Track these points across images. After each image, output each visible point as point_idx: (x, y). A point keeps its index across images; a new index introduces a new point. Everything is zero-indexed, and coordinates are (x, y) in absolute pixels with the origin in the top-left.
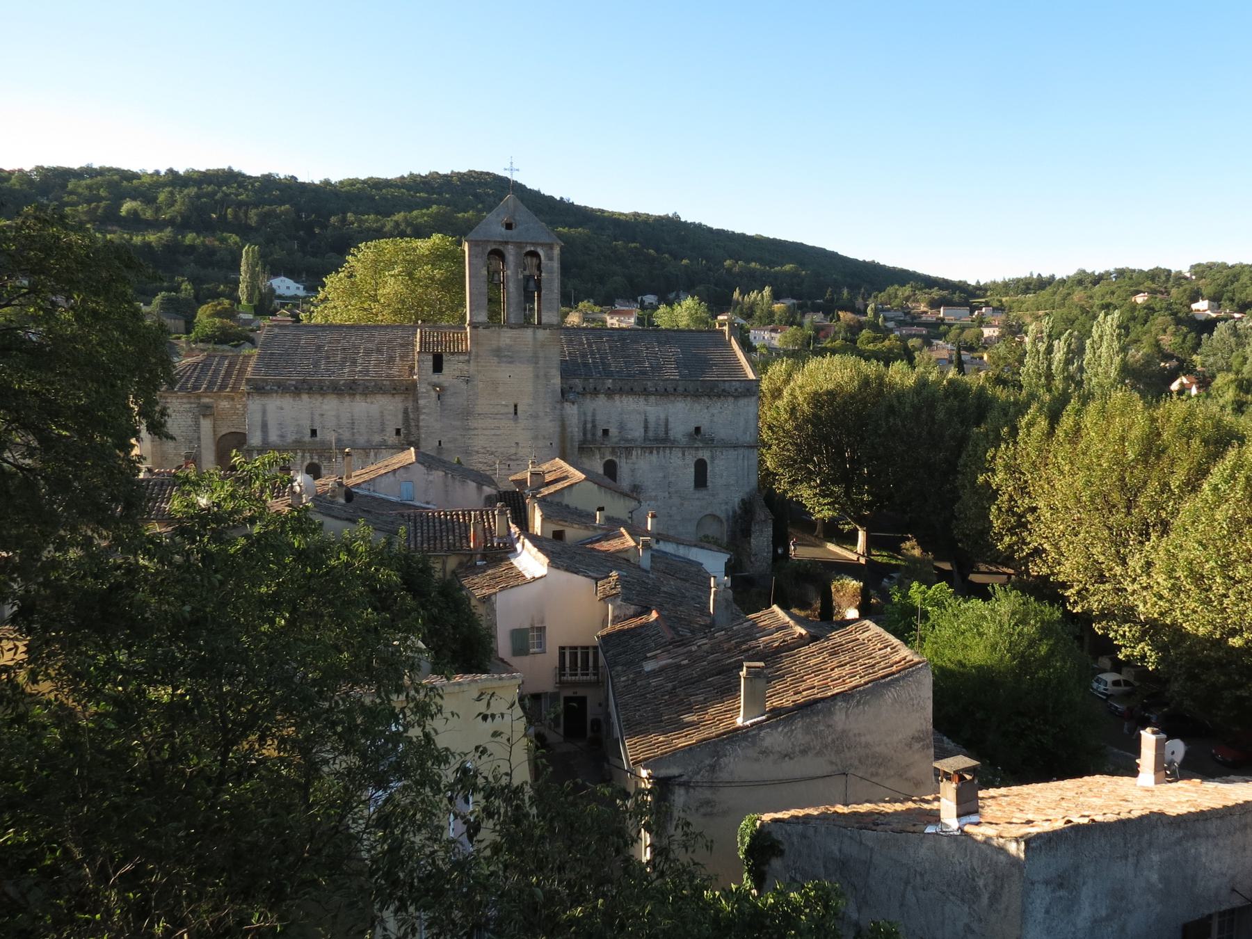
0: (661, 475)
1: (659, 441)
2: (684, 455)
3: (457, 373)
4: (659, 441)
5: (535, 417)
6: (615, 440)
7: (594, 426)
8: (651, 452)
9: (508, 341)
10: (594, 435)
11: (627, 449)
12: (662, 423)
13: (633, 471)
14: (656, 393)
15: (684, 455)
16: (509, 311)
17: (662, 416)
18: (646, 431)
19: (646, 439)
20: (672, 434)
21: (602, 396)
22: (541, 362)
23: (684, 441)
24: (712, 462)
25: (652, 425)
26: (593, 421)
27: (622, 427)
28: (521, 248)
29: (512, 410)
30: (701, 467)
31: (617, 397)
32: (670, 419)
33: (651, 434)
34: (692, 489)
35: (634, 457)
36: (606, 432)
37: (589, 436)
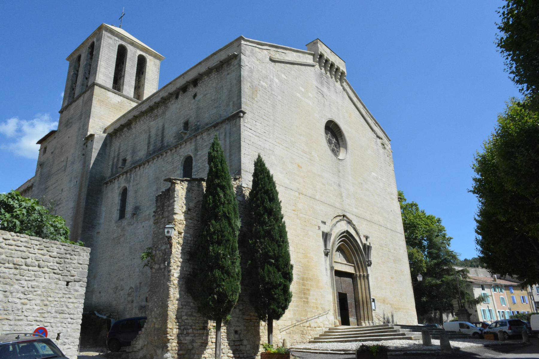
12: (160, 133)
13: (136, 192)
18: (148, 147)
24: (196, 155)
25: (152, 140)
32: (166, 126)
36: (125, 160)
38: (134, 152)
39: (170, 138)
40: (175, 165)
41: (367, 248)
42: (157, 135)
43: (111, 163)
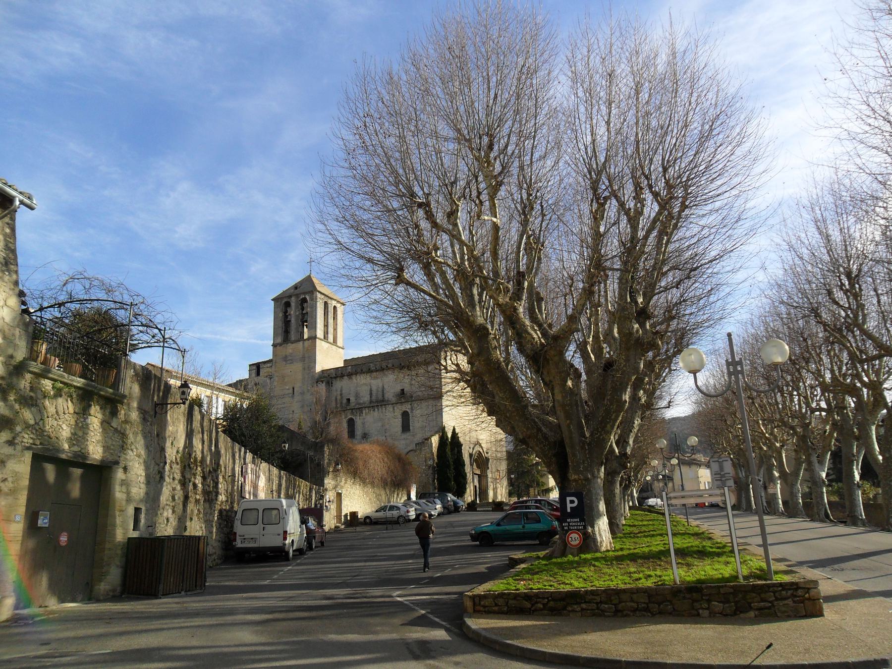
0: (380, 424)
1: (379, 402)
2: (394, 409)
3: (266, 374)
4: (379, 402)
5: (302, 393)
6: (353, 404)
7: (342, 398)
9: (290, 351)
10: (341, 403)
11: (360, 409)
12: (380, 390)
13: (363, 424)
14: (377, 371)
15: (394, 409)
16: (293, 336)
17: (381, 385)
18: (371, 397)
19: (371, 402)
20: (386, 396)
21: (346, 377)
23: (394, 400)
24: (412, 412)
25: (374, 393)
26: (341, 395)
27: (357, 396)
28: (298, 298)
29: (291, 391)
30: (405, 416)
31: (354, 377)
33: (374, 398)
34: (400, 433)
35: (364, 414)
36: (349, 400)
39: (390, 395)
40: (396, 414)
41: (487, 459)
42: (378, 391)
43: (334, 398)
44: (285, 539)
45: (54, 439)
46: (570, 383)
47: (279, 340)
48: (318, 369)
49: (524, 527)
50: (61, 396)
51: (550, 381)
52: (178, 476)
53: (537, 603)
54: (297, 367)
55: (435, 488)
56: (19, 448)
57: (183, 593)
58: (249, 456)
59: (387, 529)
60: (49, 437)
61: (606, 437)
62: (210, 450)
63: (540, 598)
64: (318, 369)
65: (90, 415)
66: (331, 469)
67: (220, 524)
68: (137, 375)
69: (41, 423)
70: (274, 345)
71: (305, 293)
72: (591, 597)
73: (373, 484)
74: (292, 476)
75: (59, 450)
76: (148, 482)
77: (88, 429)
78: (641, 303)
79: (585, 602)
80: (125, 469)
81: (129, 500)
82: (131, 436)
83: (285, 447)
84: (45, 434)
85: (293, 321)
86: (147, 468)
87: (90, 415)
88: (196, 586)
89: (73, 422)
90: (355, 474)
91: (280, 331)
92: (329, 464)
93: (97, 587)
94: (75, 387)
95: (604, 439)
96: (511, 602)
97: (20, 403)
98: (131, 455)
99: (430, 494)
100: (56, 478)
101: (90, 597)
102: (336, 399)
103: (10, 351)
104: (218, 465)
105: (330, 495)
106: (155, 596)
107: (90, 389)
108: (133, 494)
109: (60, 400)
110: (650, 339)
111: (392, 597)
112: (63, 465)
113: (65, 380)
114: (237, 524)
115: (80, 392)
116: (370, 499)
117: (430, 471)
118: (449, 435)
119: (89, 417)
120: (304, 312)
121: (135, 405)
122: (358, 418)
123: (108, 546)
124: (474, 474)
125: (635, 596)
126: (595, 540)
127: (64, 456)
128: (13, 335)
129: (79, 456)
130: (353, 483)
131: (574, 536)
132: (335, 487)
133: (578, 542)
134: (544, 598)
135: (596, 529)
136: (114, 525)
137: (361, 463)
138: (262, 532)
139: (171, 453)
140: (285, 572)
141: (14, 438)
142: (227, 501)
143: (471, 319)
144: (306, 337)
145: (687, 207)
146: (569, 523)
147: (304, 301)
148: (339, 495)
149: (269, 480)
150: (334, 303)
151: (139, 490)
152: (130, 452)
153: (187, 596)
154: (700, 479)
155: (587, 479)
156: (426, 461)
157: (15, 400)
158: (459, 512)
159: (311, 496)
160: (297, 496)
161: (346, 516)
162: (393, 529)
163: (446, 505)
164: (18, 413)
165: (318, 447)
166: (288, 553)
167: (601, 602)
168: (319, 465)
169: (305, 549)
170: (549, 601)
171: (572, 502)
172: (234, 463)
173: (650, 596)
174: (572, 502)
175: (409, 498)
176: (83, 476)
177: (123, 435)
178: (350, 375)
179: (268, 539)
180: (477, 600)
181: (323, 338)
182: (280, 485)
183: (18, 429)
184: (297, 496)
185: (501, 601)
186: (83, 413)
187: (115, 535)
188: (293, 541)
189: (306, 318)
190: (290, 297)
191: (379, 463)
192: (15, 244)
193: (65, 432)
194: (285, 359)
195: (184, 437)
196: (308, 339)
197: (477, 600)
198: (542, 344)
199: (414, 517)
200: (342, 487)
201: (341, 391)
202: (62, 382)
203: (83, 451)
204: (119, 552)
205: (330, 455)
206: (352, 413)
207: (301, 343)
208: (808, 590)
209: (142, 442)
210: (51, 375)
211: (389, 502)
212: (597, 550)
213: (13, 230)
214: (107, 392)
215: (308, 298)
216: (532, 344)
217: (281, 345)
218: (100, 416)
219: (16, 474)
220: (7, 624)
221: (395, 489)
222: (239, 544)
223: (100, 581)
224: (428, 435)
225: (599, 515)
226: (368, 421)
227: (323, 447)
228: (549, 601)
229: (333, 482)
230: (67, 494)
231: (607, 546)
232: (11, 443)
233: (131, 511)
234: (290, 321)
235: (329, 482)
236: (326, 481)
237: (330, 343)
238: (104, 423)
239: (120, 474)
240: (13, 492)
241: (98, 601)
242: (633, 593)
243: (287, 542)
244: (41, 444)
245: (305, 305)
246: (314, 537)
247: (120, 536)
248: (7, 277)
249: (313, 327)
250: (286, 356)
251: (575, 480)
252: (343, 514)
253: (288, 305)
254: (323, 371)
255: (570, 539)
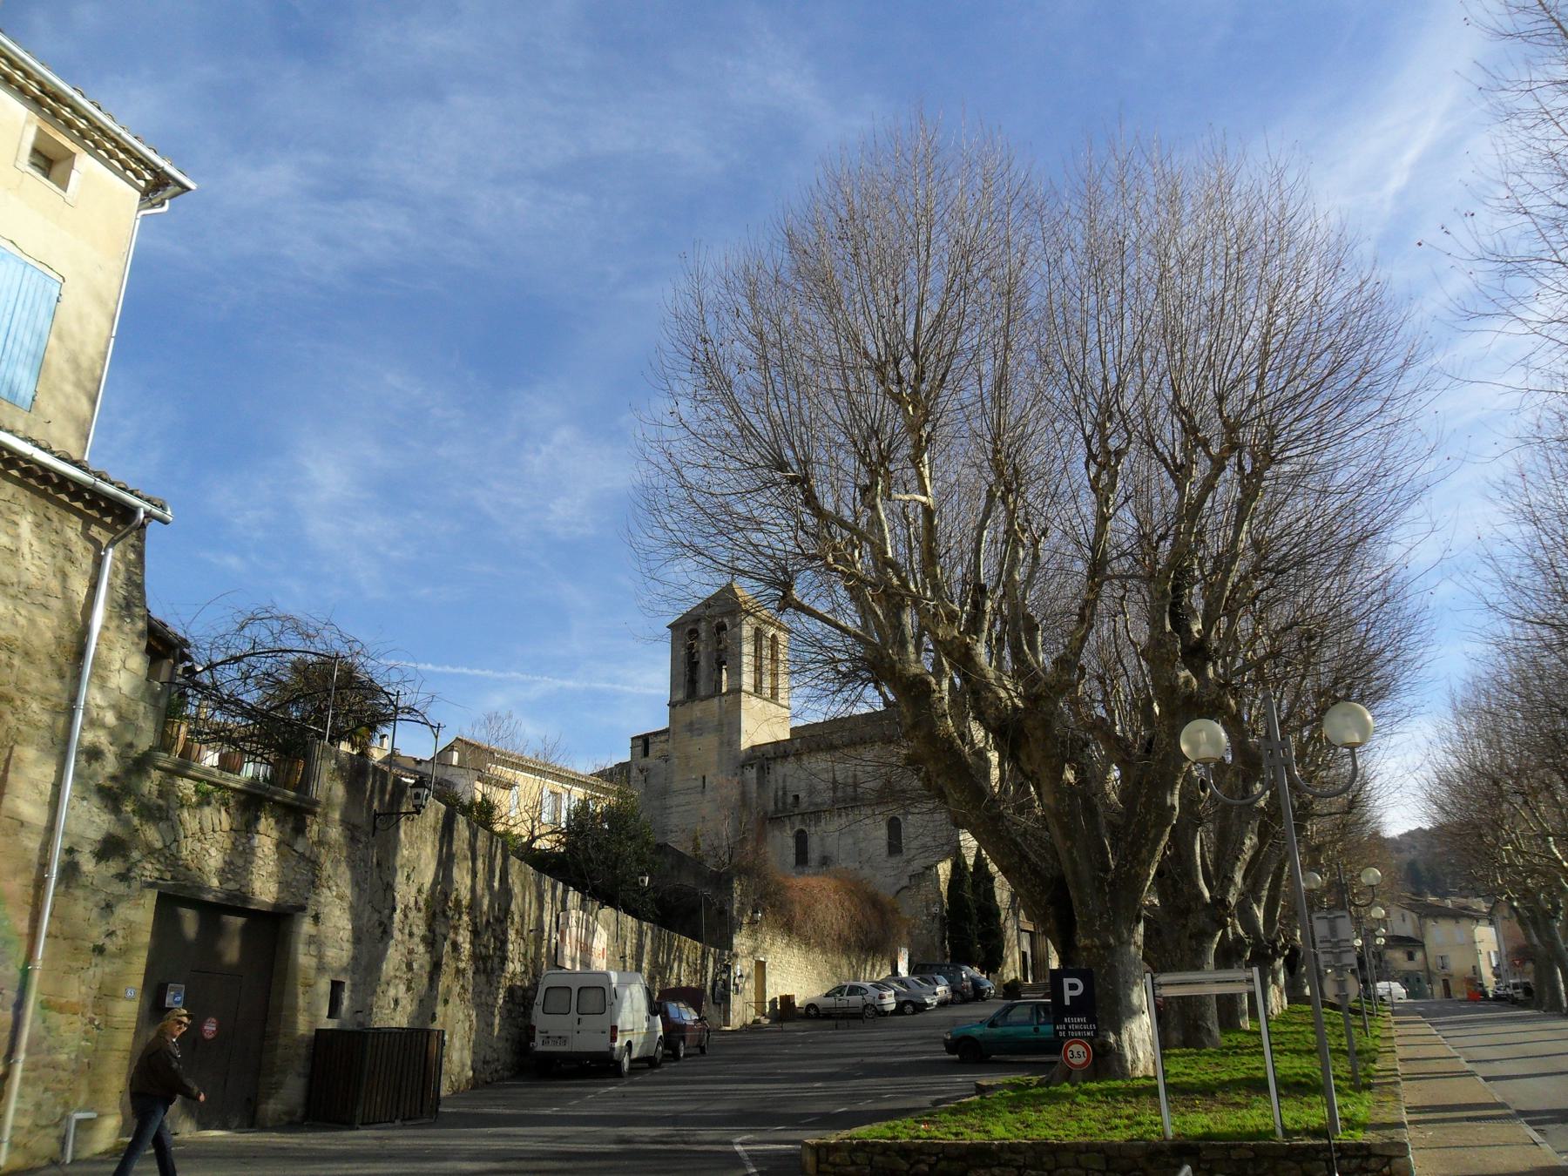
3: (659, 754)
7: (785, 793)
8: (840, 816)
9: (699, 714)
10: (784, 803)
11: (816, 814)
16: (703, 688)
21: (792, 759)
22: (725, 729)
26: (784, 788)
27: (812, 791)
28: (710, 622)
29: (700, 783)
36: (796, 797)
37: (780, 805)
38: (812, 791)
44: (614, 1039)
45: (195, 871)
46: (1069, 775)
47: (680, 696)
48: (745, 743)
49: (1036, 1030)
50: (209, 804)
51: (1033, 772)
52: (420, 930)
53: (918, 1162)
54: (710, 741)
55: (946, 957)
56: (136, 885)
57: (398, 1122)
58: (574, 897)
59: (837, 1028)
60: (187, 868)
61: (1142, 872)
62: (490, 887)
63: (923, 1154)
64: (745, 743)
65: (258, 833)
66: (746, 920)
67: (509, 1011)
68: (340, 768)
69: (174, 846)
70: (672, 705)
71: (723, 615)
72: (1008, 1156)
73: (821, 945)
74: (665, 932)
75: (202, 888)
76: (358, 938)
77: (254, 854)
78: (1199, 632)
79: (999, 1165)
80: (316, 918)
81: (321, 968)
82: (328, 865)
83: (643, 881)
84: (181, 862)
85: (703, 663)
86: (356, 916)
87: (258, 833)
88: (421, 1112)
89: (227, 844)
90: (791, 928)
91: (682, 680)
92: (741, 911)
93: (263, 1107)
94: (234, 790)
95: (1138, 875)
96: (877, 1158)
97: (141, 816)
98: (327, 895)
99: (931, 966)
100: (199, 933)
101: (252, 1122)
102: (776, 795)
103: (129, 737)
104: (506, 911)
105: (743, 966)
106: (350, 1125)
107: (258, 792)
108: (328, 959)
109: (207, 810)
110: (1214, 696)
111: (731, 1143)
112: (212, 913)
113: (216, 780)
114: (537, 1011)
115: (242, 797)
116: (819, 974)
117: (937, 925)
118: (970, 861)
119: (257, 836)
120: (722, 646)
121: (337, 816)
122: (813, 829)
123: (282, 1041)
124: (1020, 930)
125: (1082, 1158)
126: (1121, 1057)
127: (210, 897)
128: (135, 712)
129: (236, 897)
130: (788, 945)
131: (1076, 1048)
132: (753, 952)
133: (1083, 1060)
134: (930, 1155)
135: (1125, 1037)
136: (294, 1009)
137: (798, 909)
138: (577, 1027)
139: (405, 893)
140: (601, 1096)
141: (129, 870)
142: (525, 972)
143: (899, 666)
144: (724, 690)
145: (1273, 459)
146: (1067, 1024)
147: (721, 628)
148: (761, 966)
149: (617, 937)
150: (772, 631)
151: (339, 951)
152: (325, 891)
153: (404, 1127)
154: (1479, 946)
155: (1107, 946)
156: (927, 907)
157: (133, 811)
158: (984, 1000)
159: (705, 967)
160: (676, 965)
161: (773, 1002)
162: (849, 1027)
163: (959, 987)
164: (137, 830)
165: (721, 881)
166: (619, 1063)
167: (1026, 1166)
168: (722, 912)
169: (659, 1057)
170: (939, 1160)
171: (1073, 987)
172: (541, 908)
173: (1108, 1159)
174: (1073, 987)
175: (895, 971)
176: (245, 930)
177: (314, 864)
178: (798, 755)
179: (587, 1041)
180: (823, 1154)
181: (752, 690)
182: (640, 947)
183: (136, 855)
184: (676, 965)
185: (860, 1157)
186: (245, 829)
187: (295, 1023)
188: (629, 1044)
189: (725, 658)
190: (698, 621)
191: (833, 910)
192: (143, 575)
193: (214, 859)
194: (691, 727)
195: (433, 866)
196: (729, 692)
197: (823, 1154)
198: (1015, 706)
199: (893, 1007)
200: (766, 952)
201: (784, 781)
202: (209, 783)
203: (244, 890)
204: (303, 1051)
205: (744, 894)
206: (803, 821)
207: (716, 700)
208: (1389, 1159)
209: (348, 875)
210: (191, 773)
211: (856, 978)
212: (1124, 1074)
213: (141, 555)
214: (285, 795)
215: (726, 620)
216: (997, 708)
217: (682, 703)
218: (275, 834)
219: (130, 926)
220: (104, 1157)
221: (867, 956)
222: (539, 1045)
223: (269, 1096)
224: (930, 862)
225: (1133, 1012)
226: (828, 835)
227: (730, 881)
228: (939, 1160)
229: (749, 943)
230: (218, 956)
231: (1146, 1068)
232: (123, 877)
233: (324, 986)
234: (698, 663)
235: (741, 942)
236: (736, 941)
237: (765, 699)
238: (282, 846)
239: (306, 927)
240: (124, 952)
241: (264, 1128)
242: (1081, 1152)
243: (617, 1044)
244: (173, 878)
245: (723, 635)
246: (683, 1038)
247: (303, 1026)
248: (129, 626)
249: (736, 672)
250: (691, 724)
251: (1085, 948)
252: (768, 999)
253: (694, 633)
254: (753, 748)
255: (1069, 1054)
